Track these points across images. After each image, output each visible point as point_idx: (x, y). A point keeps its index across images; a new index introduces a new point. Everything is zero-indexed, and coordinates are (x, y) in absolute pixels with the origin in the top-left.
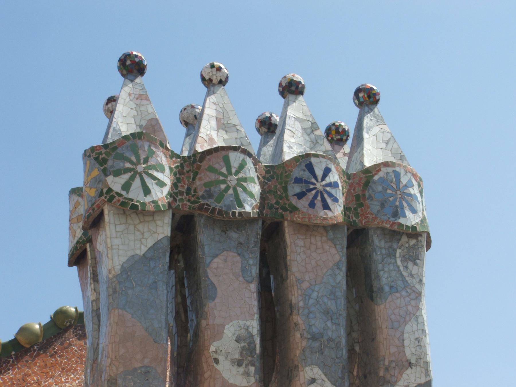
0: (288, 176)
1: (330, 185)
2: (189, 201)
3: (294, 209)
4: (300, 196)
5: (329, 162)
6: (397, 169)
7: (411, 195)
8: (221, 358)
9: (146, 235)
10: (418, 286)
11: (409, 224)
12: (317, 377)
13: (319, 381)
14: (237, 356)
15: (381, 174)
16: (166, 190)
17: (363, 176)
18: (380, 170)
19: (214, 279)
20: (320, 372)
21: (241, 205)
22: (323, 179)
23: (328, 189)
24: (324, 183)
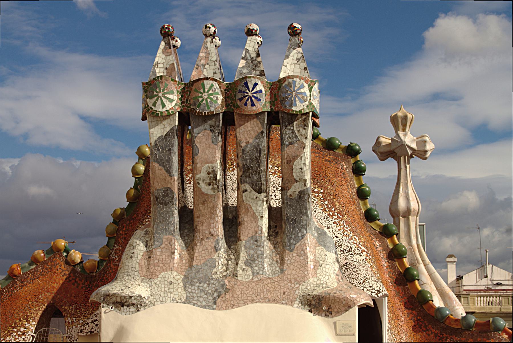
0: (236, 89)
1: (256, 92)
2: (187, 106)
3: (238, 107)
4: (241, 99)
5: (257, 79)
6: (295, 79)
7: (301, 93)
8: (201, 182)
9: (166, 126)
10: (304, 140)
11: (297, 110)
12: (248, 189)
13: (249, 191)
14: (208, 181)
15: (286, 83)
16: (174, 103)
17: (278, 84)
18: (285, 81)
19: (198, 145)
20: (249, 187)
21: (209, 108)
22: (253, 90)
23: (255, 95)
24: (253, 92)
